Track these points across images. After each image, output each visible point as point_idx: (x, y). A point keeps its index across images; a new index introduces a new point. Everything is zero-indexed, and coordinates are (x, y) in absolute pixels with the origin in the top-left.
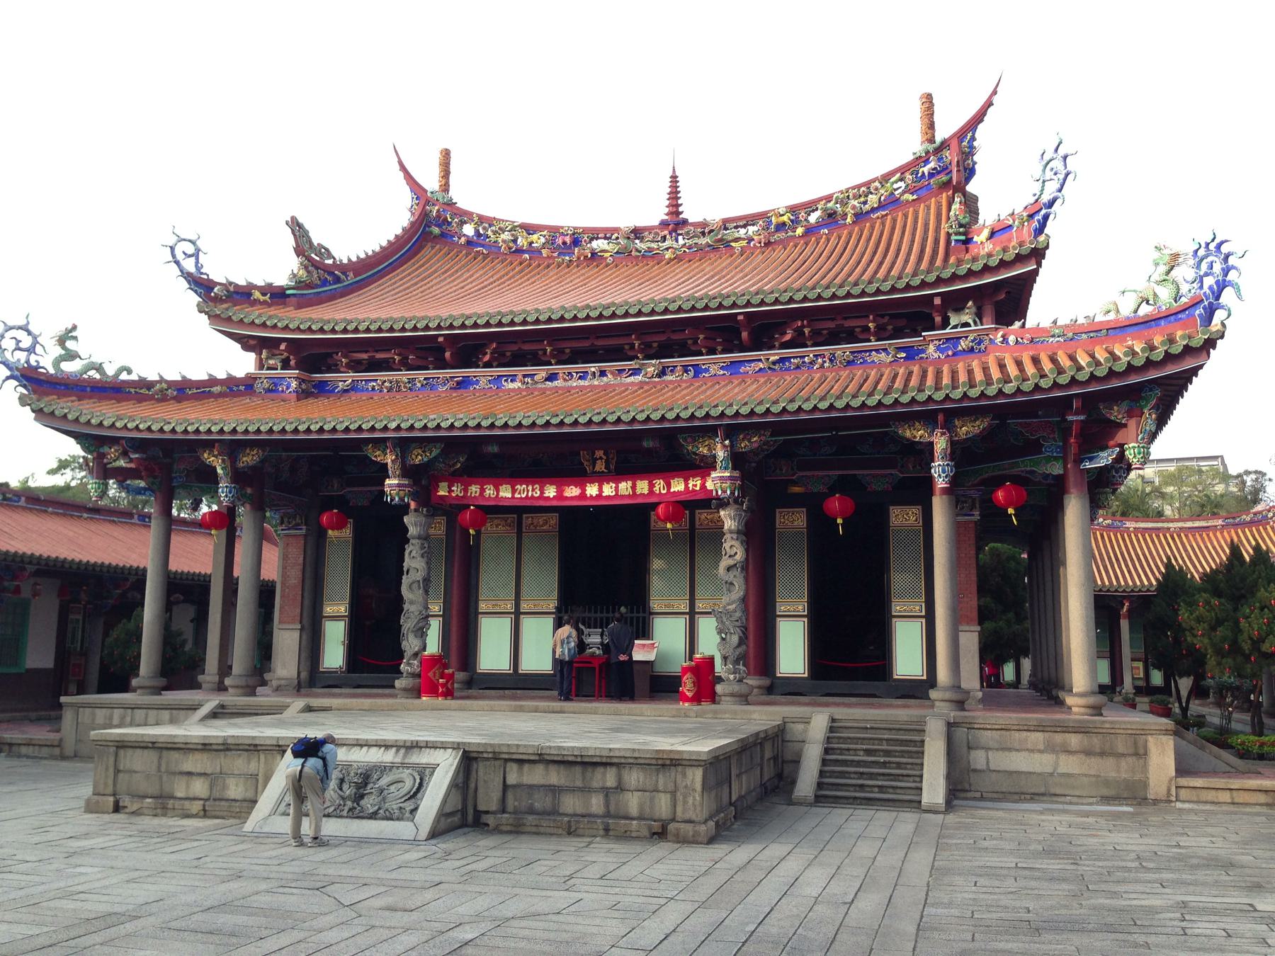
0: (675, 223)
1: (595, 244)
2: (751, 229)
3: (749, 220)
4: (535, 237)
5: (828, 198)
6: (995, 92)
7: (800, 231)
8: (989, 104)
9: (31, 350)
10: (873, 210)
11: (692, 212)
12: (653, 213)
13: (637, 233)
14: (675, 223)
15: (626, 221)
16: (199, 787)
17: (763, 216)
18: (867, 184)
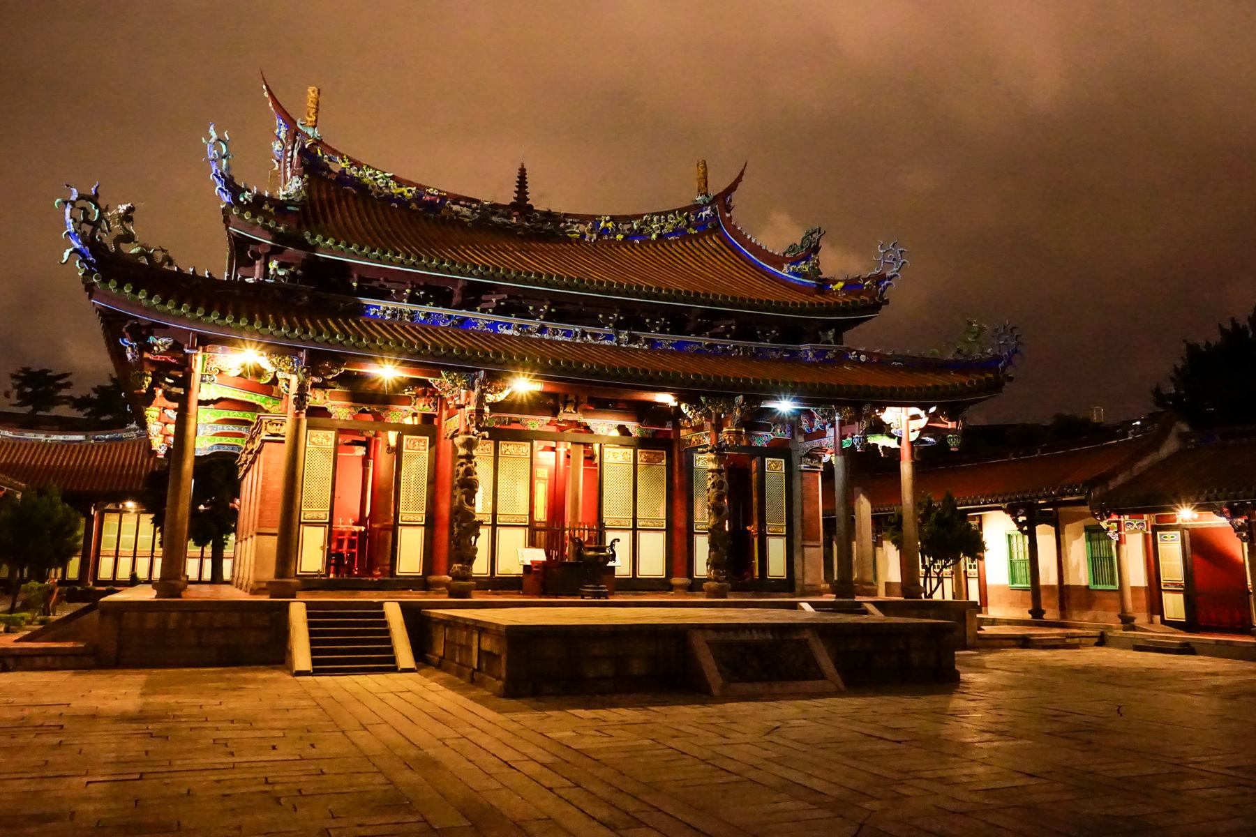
0: (521, 204)
1: (455, 208)
2: (582, 228)
3: (583, 219)
4: (404, 190)
5: (641, 216)
6: (742, 174)
7: (620, 237)
8: (739, 179)
9: (96, 225)
10: (670, 234)
11: (540, 201)
12: (507, 196)
13: (495, 207)
14: (521, 204)
15: (486, 198)
16: (606, 669)
17: (595, 219)
18: (666, 214)
